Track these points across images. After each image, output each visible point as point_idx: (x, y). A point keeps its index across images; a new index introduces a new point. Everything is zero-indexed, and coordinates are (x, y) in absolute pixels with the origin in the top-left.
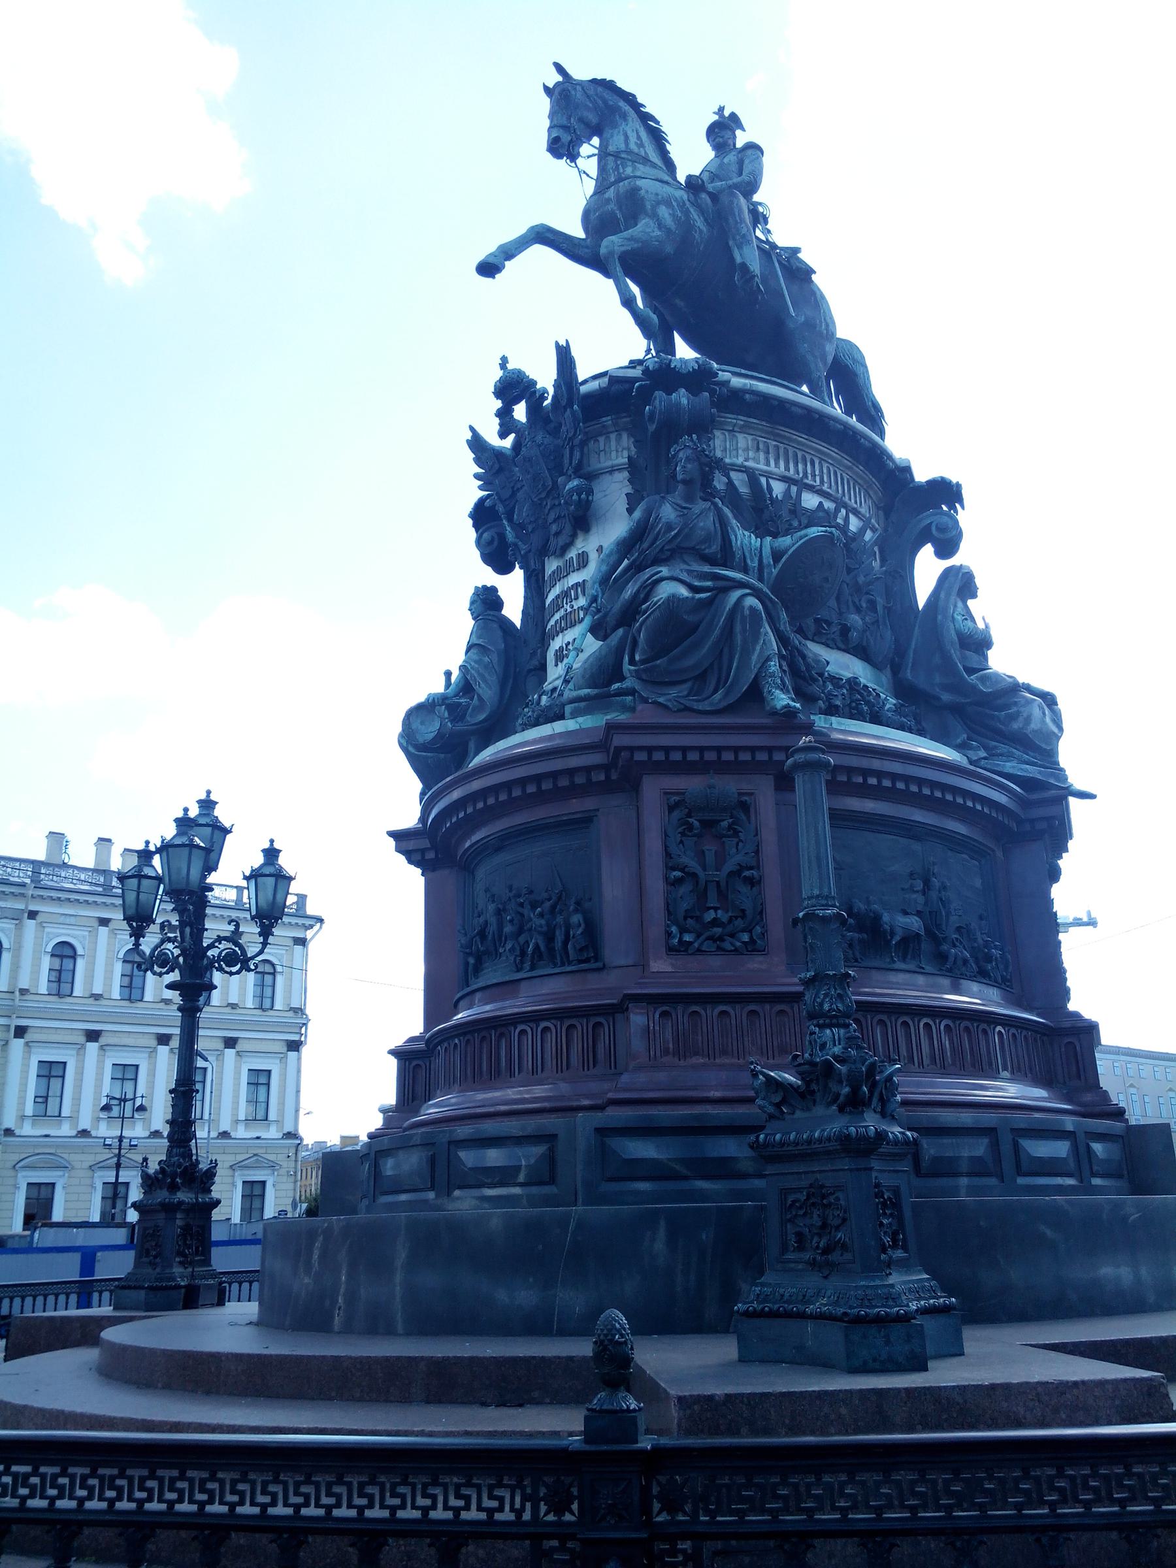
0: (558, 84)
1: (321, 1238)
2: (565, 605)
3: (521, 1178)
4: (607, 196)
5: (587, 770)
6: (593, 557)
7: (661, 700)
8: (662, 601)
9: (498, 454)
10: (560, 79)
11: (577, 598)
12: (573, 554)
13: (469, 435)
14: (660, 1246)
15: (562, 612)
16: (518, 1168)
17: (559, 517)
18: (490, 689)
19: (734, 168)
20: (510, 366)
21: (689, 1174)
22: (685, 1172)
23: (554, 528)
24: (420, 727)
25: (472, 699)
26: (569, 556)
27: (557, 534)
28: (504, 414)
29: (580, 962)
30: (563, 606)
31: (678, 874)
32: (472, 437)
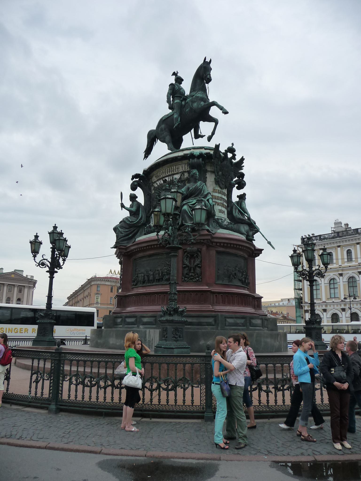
0: (207, 62)
20: (234, 147)
23: (223, 183)
28: (227, 151)
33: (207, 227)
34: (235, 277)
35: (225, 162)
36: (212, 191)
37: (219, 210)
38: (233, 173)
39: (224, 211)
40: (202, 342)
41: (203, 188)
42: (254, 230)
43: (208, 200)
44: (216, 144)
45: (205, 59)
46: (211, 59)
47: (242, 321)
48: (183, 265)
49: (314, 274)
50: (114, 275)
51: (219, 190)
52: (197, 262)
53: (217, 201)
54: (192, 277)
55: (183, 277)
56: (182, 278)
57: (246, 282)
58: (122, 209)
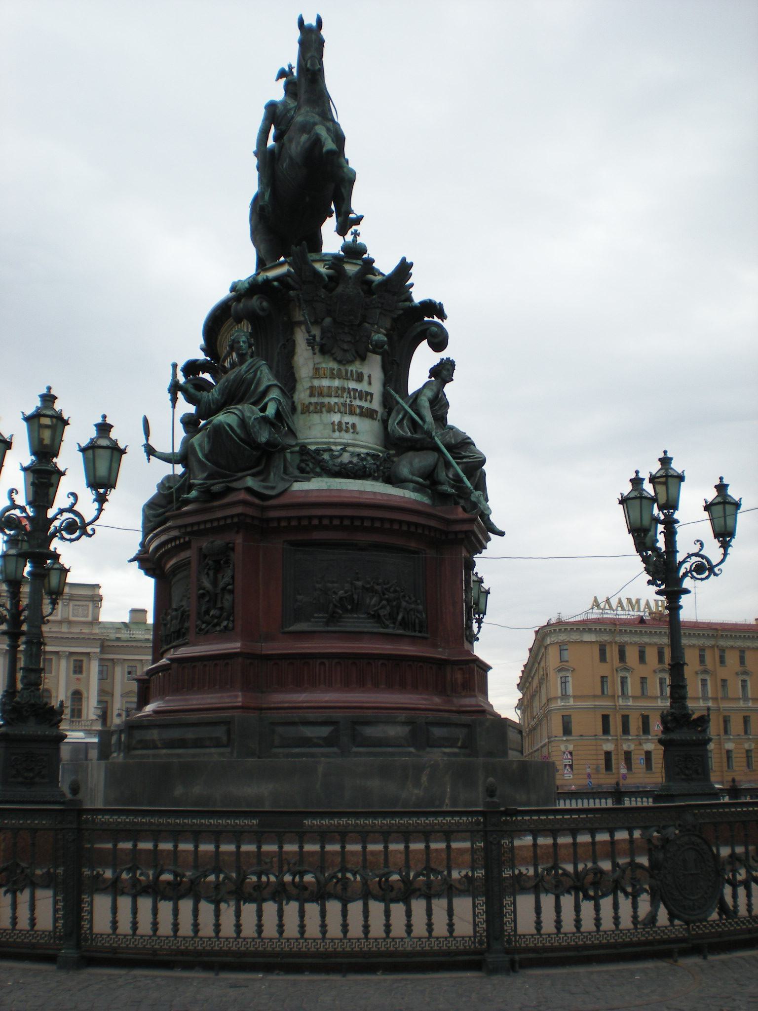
2: (345, 398)
3: (459, 744)
6: (366, 378)
8: (480, 459)
11: (355, 398)
15: (342, 400)
17: (350, 342)
20: (360, 240)
23: (346, 347)
33: (250, 482)
34: (349, 607)
35: (340, 289)
36: (311, 375)
37: (333, 423)
38: (378, 311)
39: (354, 426)
40: (179, 791)
41: (255, 375)
43: (263, 409)
47: (325, 731)
48: (199, 589)
49: (682, 571)
50: (606, 611)
51: (334, 369)
52: (227, 579)
53: (326, 400)
54: (216, 621)
55: (199, 622)
56: (197, 626)
57: (400, 617)
58: (149, 459)
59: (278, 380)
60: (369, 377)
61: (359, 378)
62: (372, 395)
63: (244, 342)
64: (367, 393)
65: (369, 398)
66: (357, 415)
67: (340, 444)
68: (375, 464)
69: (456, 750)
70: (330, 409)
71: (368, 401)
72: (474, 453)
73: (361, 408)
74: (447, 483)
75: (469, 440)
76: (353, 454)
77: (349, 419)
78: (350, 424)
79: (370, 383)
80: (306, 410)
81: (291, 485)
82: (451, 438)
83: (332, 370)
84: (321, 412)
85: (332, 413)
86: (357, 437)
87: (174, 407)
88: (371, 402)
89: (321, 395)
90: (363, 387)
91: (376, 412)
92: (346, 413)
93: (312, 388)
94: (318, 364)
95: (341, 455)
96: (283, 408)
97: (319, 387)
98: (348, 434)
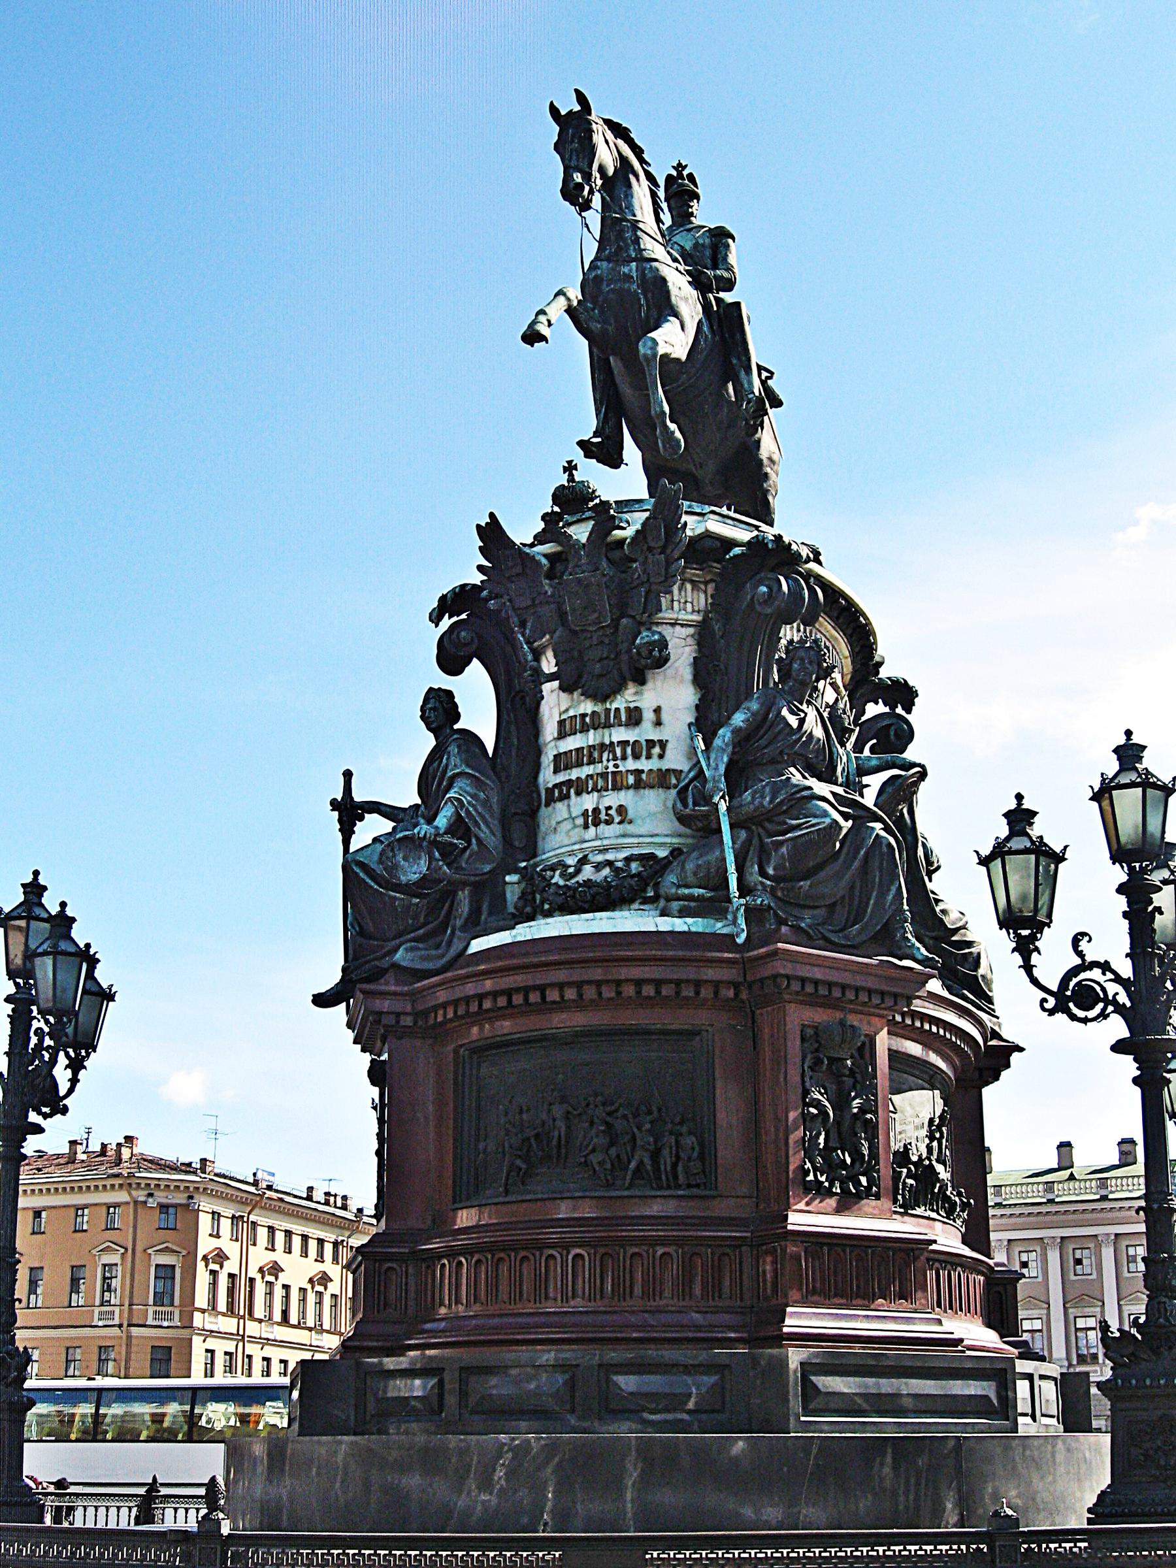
1: (510, 1455)
2: (605, 763)
3: (691, 1405)
4: (626, 270)
5: (717, 985)
6: (648, 716)
7: (803, 925)
9: (519, 554)
10: (577, 108)
11: (624, 758)
12: (619, 703)
13: (484, 520)
14: (887, 1470)
15: (599, 768)
16: (690, 1395)
18: (494, 834)
19: (708, 253)
20: (578, 476)
21: (868, 1408)
22: (865, 1406)
24: (402, 863)
25: (469, 843)
26: (614, 706)
27: (601, 676)
29: (689, 1186)
30: (601, 762)
31: (813, 1110)
32: (487, 524)
36: (556, 735)
39: (621, 810)
42: (782, 843)
44: (478, 526)
45: (554, 110)
46: (577, 91)
53: (574, 774)
59: (468, 765)
60: (657, 711)
61: (634, 717)
62: (663, 744)
63: (431, 709)
64: (651, 744)
65: (656, 750)
66: (628, 788)
67: (571, 853)
68: (639, 874)
69: (685, 1416)
70: (580, 787)
71: (655, 757)
72: (815, 816)
73: (638, 772)
74: (760, 887)
75: (805, 793)
76: (598, 867)
77: (612, 799)
78: (614, 808)
79: (658, 723)
80: (550, 800)
81: (468, 944)
82: (763, 797)
83: (584, 716)
84: (568, 797)
85: (585, 795)
86: (629, 828)
87: (346, 843)
88: (661, 756)
89: (567, 767)
90: (646, 732)
91: (678, 773)
92: (607, 790)
93: (557, 757)
94: (564, 712)
95: (578, 871)
96: (468, 811)
97: (565, 753)
98: (612, 825)
